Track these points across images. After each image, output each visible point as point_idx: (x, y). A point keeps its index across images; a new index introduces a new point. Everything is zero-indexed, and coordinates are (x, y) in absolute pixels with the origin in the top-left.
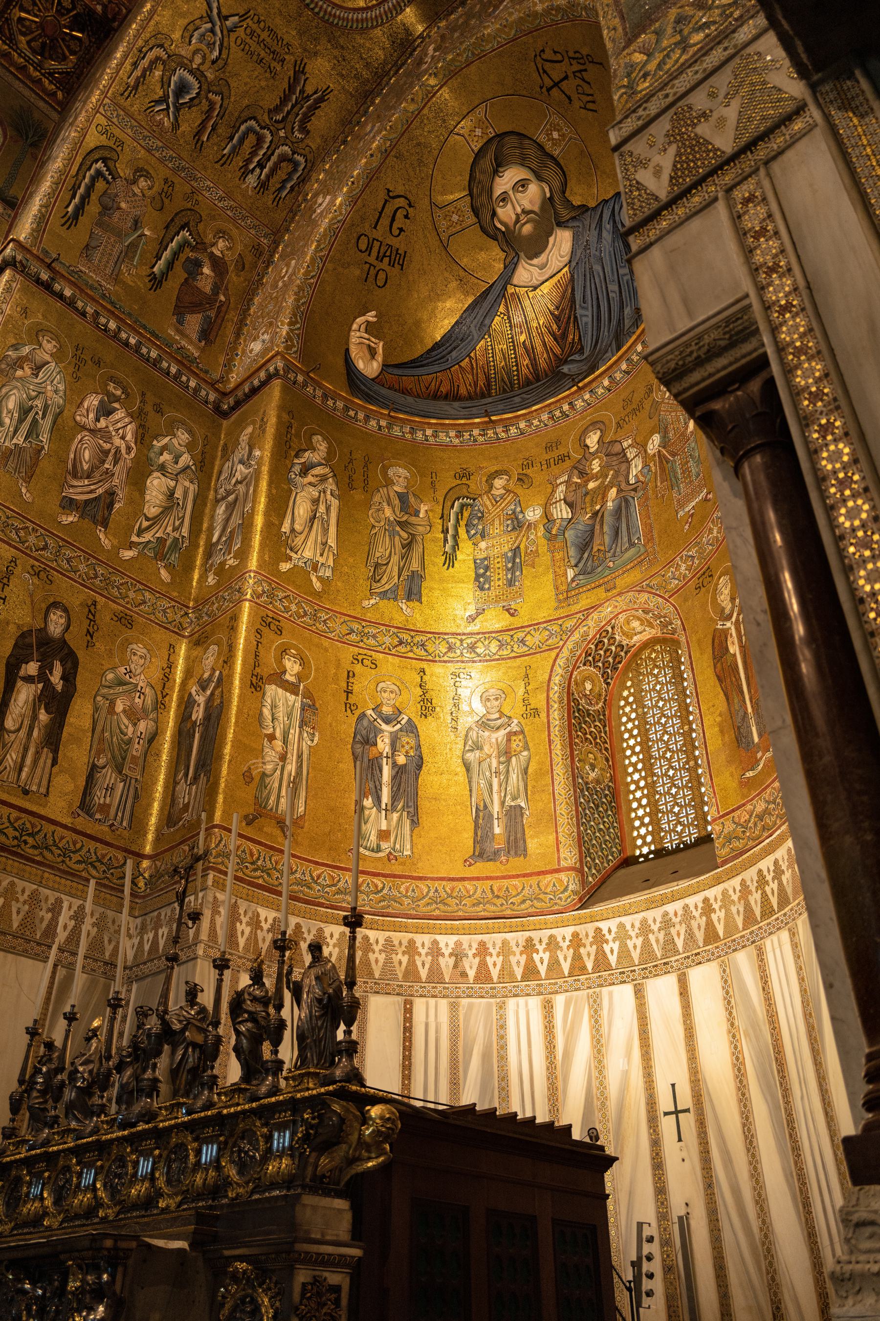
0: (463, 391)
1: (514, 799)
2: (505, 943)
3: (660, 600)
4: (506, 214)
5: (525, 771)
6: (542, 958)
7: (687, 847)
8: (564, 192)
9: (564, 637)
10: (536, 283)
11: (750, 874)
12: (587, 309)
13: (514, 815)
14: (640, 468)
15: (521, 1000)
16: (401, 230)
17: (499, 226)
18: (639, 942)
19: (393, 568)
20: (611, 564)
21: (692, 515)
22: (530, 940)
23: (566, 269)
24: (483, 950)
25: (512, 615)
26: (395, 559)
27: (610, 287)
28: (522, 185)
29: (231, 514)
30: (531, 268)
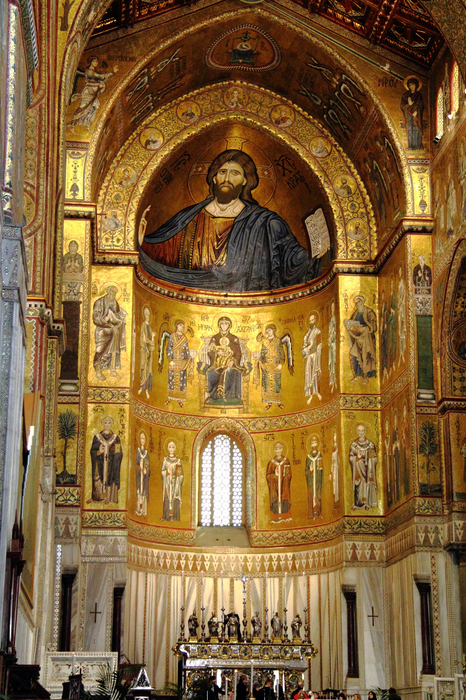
0: (167, 259)
1: (177, 495)
2: (172, 554)
3: (246, 431)
4: (221, 177)
5: (181, 484)
6: (183, 562)
7: (224, 526)
8: (252, 189)
9: (201, 427)
10: (215, 215)
11: (267, 556)
12: (234, 246)
13: (176, 502)
14: (247, 361)
15: (176, 577)
16: (179, 168)
17: (214, 180)
18: (217, 564)
19: (145, 371)
20: (225, 400)
21: (270, 406)
22: (179, 555)
23: (233, 219)
24: (165, 557)
25: (181, 407)
26: (146, 365)
27: (250, 246)
28: (237, 172)
29: (110, 341)
30: (217, 207)
